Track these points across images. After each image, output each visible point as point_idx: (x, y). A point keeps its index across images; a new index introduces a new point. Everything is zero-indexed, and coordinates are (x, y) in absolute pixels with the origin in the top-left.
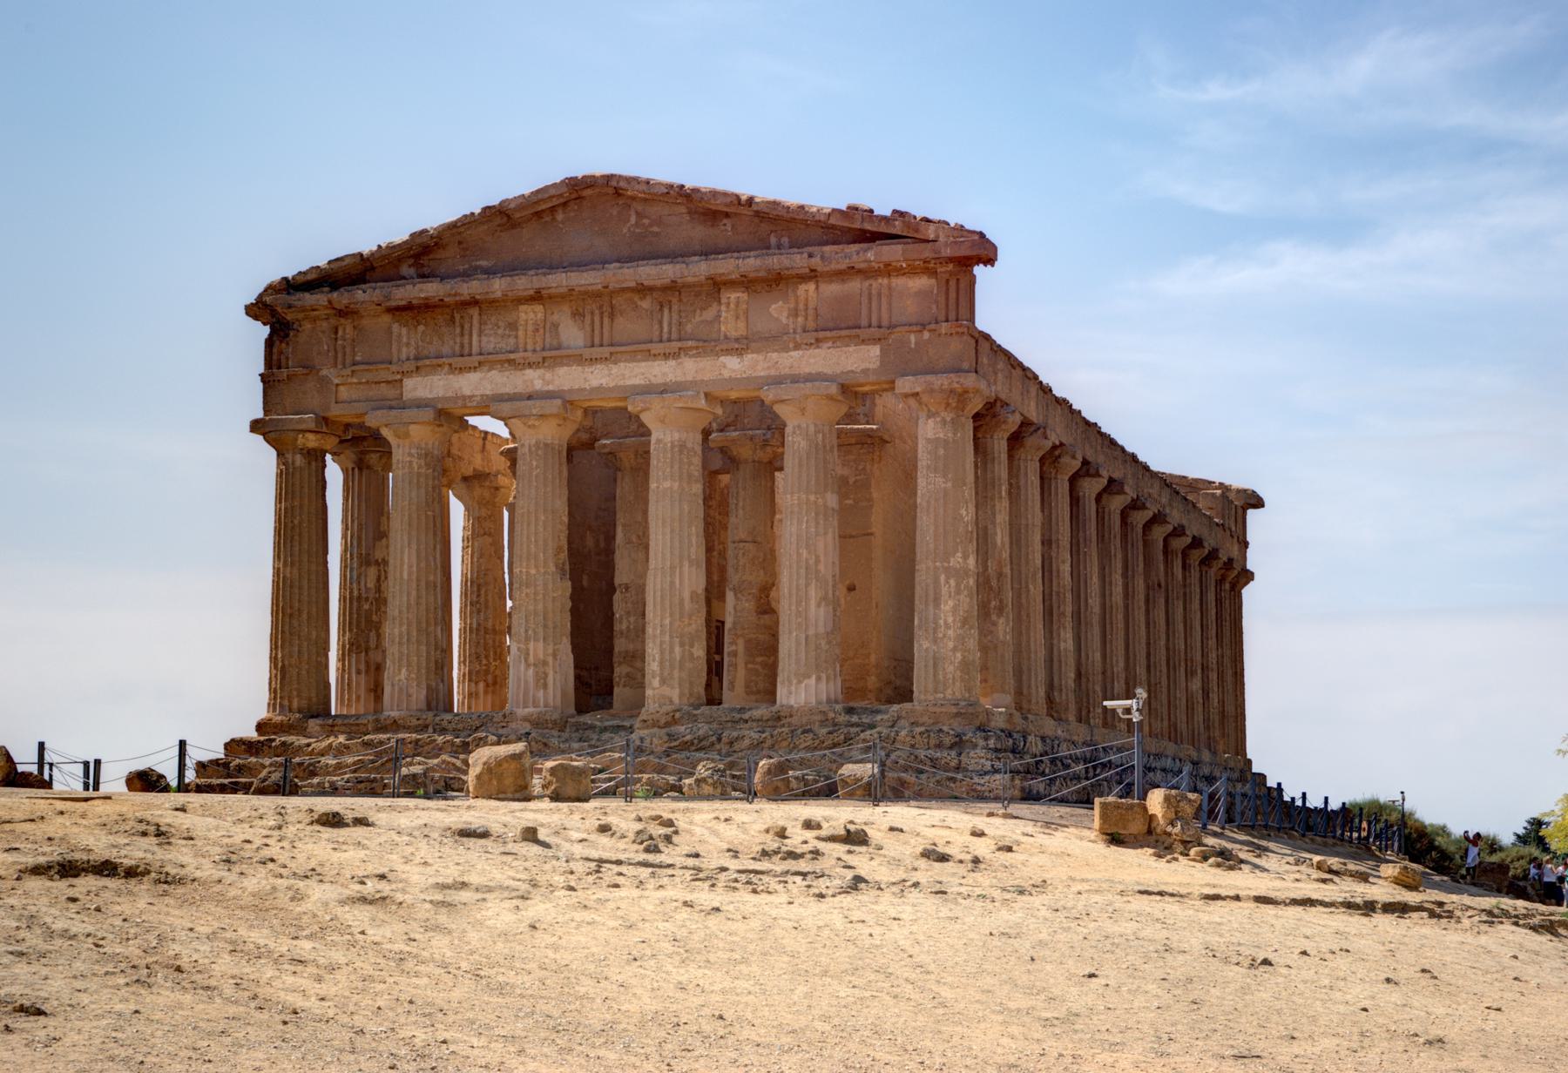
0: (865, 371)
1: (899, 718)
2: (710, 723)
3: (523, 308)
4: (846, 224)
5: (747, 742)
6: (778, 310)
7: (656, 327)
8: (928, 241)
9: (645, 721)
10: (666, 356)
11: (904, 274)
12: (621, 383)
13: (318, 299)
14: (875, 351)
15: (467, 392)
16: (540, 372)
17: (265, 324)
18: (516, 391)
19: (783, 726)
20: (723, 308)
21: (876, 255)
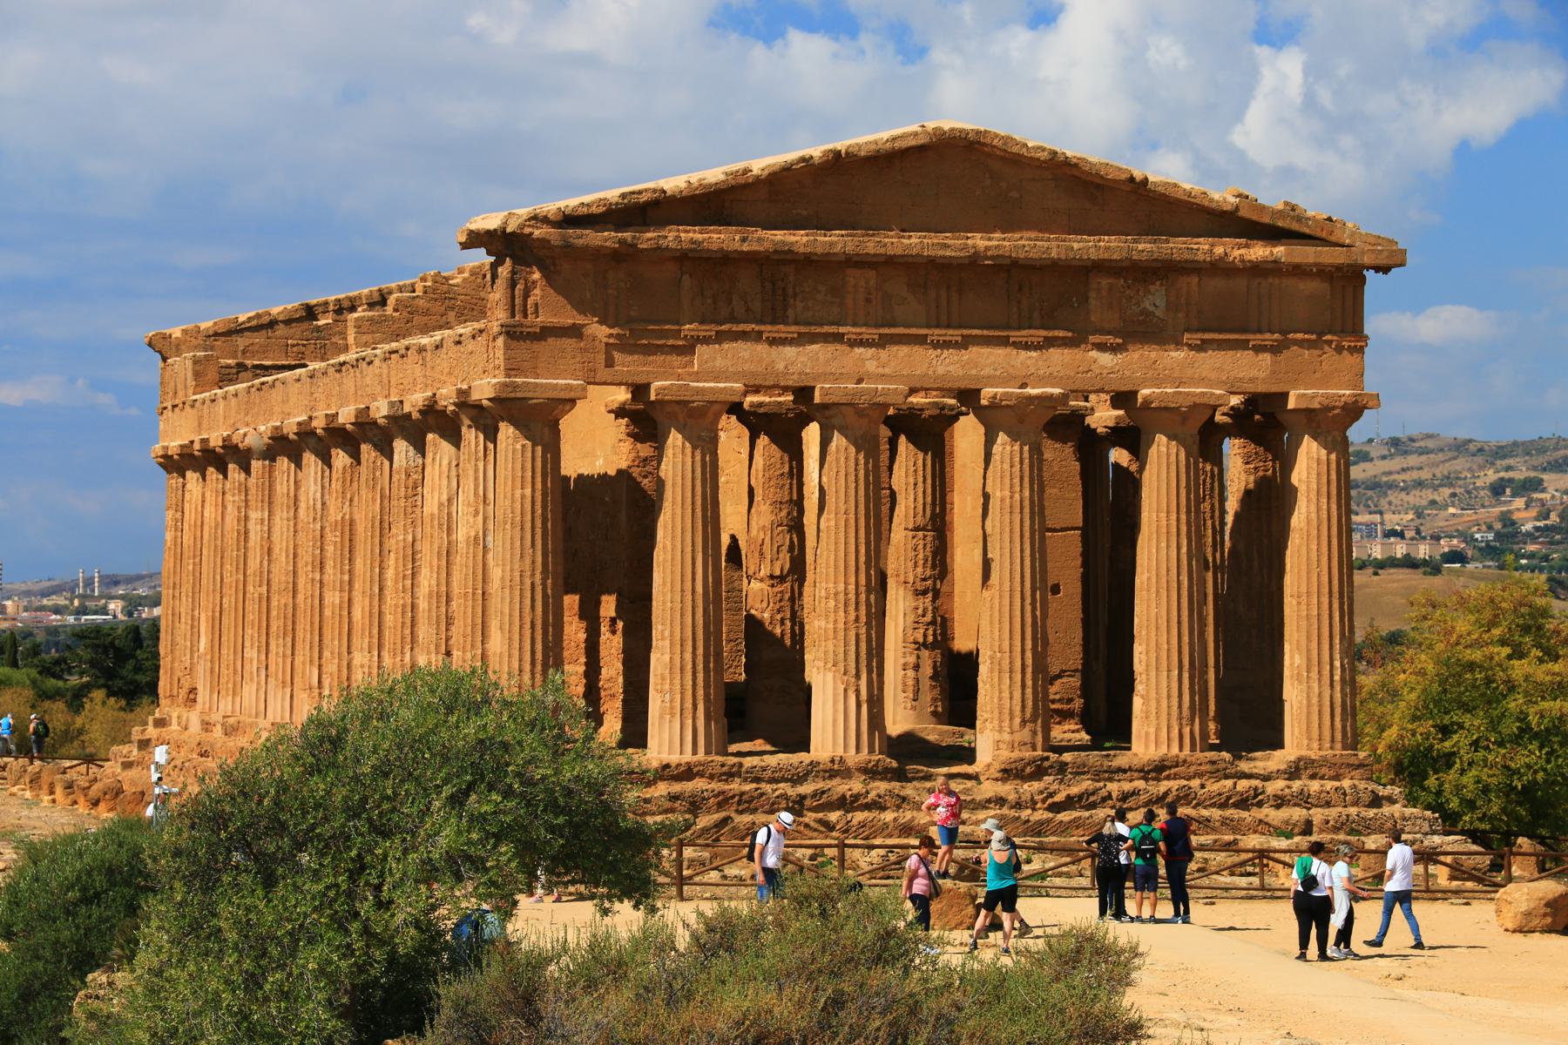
0: (1251, 380)
1: (1297, 769)
2: (1084, 773)
3: (851, 271)
4: (1254, 217)
5: (1143, 798)
6: (1155, 300)
7: (1015, 309)
8: (1343, 246)
9: (1004, 771)
10: (1027, 347)
11: (1295, 275)
12: (974, 372)
13: (606, 238)
14: (1266, 358)
15: (780, 366)
16: (871, 351)
17: (489, 253)
18: (843, 371)
19: (1168, 778)
20: (1092, 294)
21: (1287, 254)
